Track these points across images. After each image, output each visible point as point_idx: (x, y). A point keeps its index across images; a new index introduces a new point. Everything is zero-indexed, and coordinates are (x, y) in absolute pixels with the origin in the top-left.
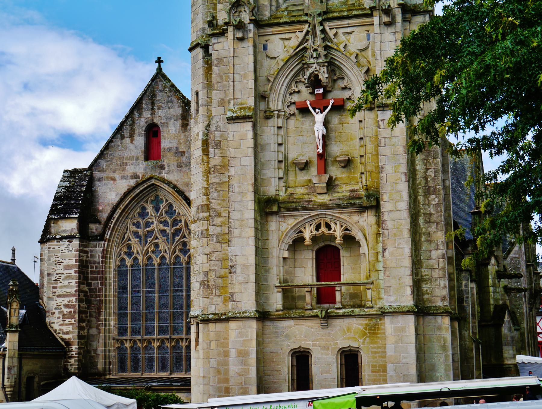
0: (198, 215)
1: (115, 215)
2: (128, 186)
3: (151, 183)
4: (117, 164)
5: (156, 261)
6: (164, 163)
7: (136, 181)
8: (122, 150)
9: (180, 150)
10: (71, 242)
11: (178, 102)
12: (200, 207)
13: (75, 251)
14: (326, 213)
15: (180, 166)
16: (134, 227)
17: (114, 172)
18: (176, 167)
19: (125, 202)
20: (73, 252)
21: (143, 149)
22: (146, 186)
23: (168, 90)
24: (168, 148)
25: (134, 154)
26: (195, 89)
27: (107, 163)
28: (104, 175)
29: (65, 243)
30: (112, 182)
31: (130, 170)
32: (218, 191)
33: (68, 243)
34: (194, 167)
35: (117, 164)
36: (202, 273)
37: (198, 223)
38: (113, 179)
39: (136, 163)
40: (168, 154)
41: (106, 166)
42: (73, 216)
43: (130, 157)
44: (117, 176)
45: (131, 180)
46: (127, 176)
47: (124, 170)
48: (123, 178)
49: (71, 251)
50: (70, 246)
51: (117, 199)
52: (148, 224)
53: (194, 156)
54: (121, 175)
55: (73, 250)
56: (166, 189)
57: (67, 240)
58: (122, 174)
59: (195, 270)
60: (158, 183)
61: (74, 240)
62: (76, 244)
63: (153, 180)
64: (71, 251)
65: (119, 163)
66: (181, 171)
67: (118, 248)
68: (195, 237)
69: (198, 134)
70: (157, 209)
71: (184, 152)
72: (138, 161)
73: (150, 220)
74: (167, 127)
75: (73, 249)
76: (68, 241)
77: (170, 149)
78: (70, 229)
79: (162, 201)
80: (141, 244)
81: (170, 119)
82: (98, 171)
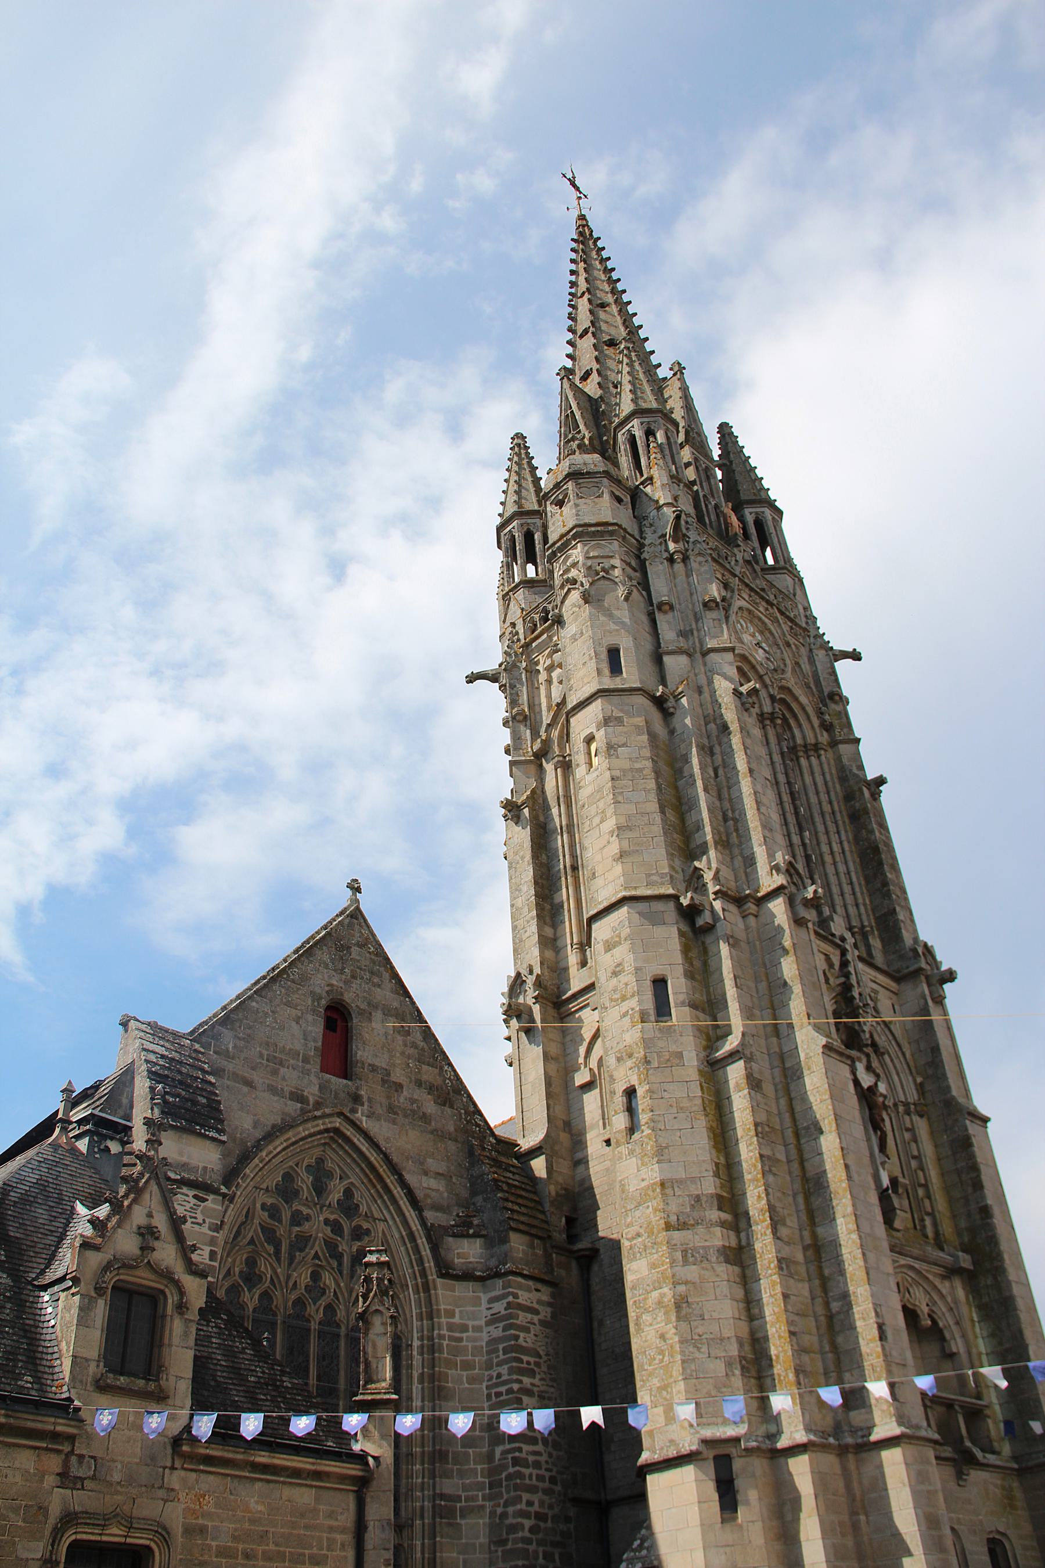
0: (695, 1214)
1: (247, 1171)
2: (283, 1113)
3: (333, 1125)
4: (261, 1056)
5: (316, 1313)
6: (363, 1093)
7: (302, 1109)
8: (273, 1028)
9: (393, 1078)
10: (204, 1200)
11: (390, 981)
12: (704, 1199)
13: (210, 1229)
14: (917, 1266)
15: (391, 1109)
16: (266, 1214)
17: (253, 1069)
18: (385, 1109)
19: (275, 1149)
20: (205, 1229)
21: (320, 1044)
22: (322, 1127)
23: (372, 949)
24: (370, 1065)
25: (298, 1046)
26: (656, 969)
27: (238, 1042)
28: (230, 1066)
29: (187, 1198)
30: (245, 1089)
31: (290, 1078)
32: (774, 1175)
33: (194, 1201)
34: (671, 1117)
35: (261, 1056)
36: (734, 1340)
37: (700, 1229)
38: (249, 1084)
39: (303, 1067)
40: (371, 1077)
41: (235, 1047)
42: (211, 1134)
43: (290, 1050)
44: (258, 1078)
45: (289, 1103)
46: (282, 1089)
47: (275, 1072)
48: (273, 1090)
49: (200, 1224)
50: (198, 1212)
51: (258, 1134)
52: (297, 1219)
53: (665, 1095)
54: (267, 1082)
55: (207, 1225)
56: (364, 1149)
57: (191, 1193)
58: (271, 1082)
59: (700, 1330)
60: (349, 1131)
61: (211, 1197)
62: (214, 1210)
63: (339, 1120)
64: (200, 1224)
65: (265, 1053)
66: (394, 1122)
67: (228, 1256)
68: (691, 1260)
69: (680, 1055)
70: (320, 1189)
71: (401, 1086)
72: (308, 1066)
73: (305, 1211)
74: (370, 1020)
75: (207, 1220)
76: (195, 1197)
77: (374, 1068)
78: (201, 1165)
79: (330, 1175)
80: (278, 1260)
81: (376, 1007)
82: (215, 1052)
